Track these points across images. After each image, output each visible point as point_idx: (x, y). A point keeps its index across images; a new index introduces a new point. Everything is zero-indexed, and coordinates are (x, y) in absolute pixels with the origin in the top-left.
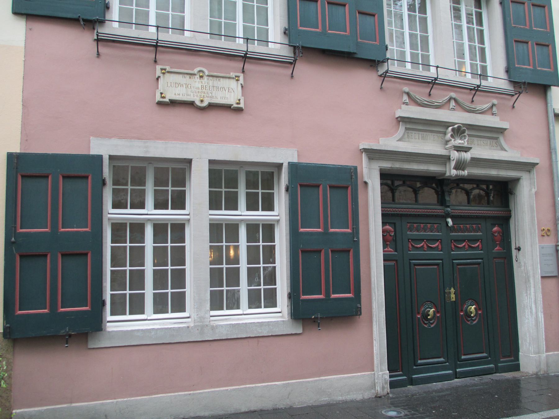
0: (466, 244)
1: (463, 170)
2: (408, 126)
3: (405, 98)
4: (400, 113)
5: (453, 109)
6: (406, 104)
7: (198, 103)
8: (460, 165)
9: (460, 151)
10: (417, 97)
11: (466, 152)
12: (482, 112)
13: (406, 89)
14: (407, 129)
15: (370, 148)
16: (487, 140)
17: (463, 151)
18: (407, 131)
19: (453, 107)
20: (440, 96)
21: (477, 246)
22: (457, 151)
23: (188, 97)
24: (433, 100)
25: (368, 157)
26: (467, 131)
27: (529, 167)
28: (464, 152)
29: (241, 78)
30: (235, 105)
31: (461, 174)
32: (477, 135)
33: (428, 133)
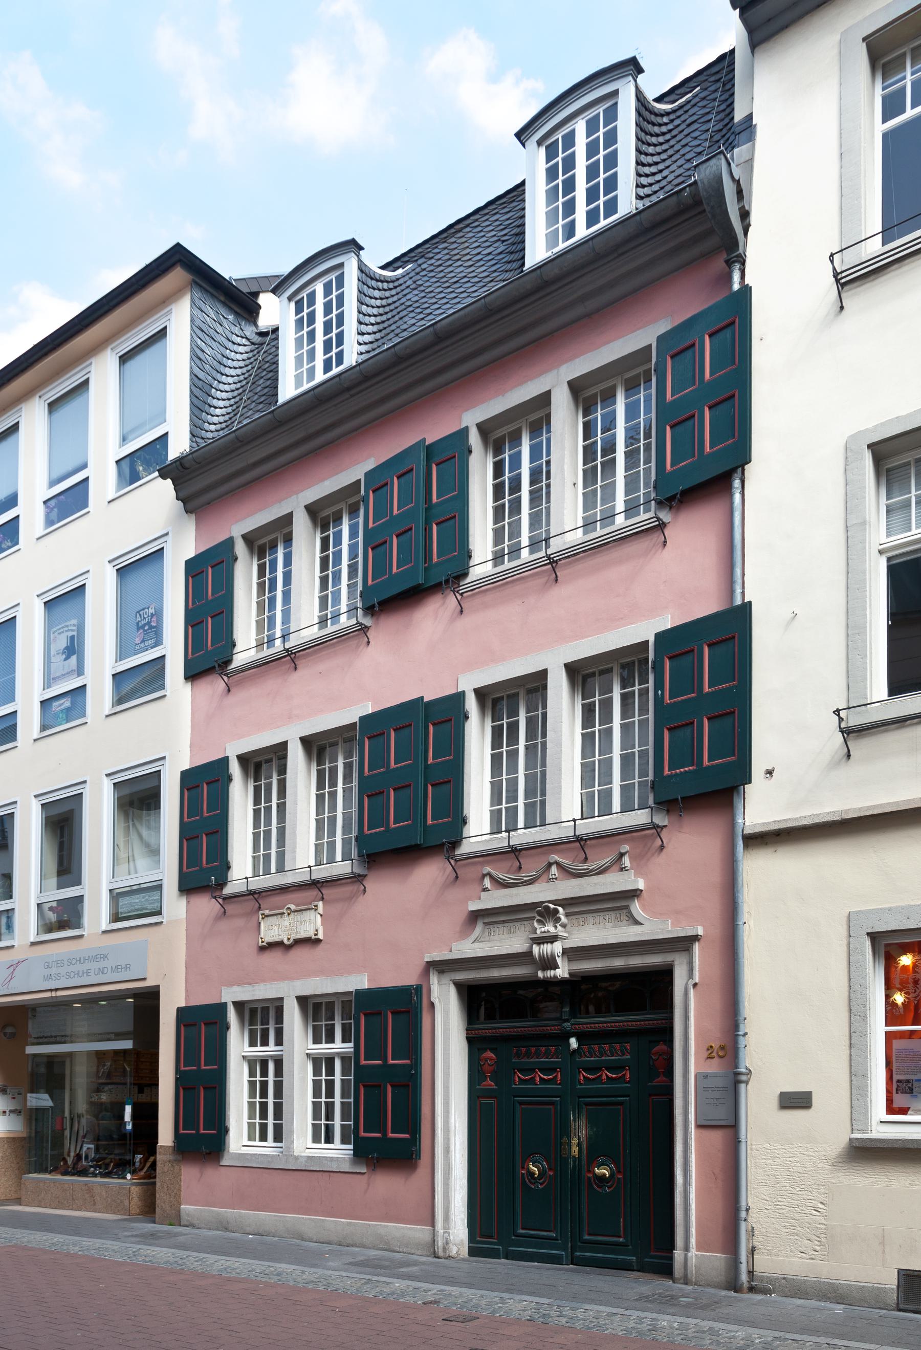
0: (604, 1074)
1: (555, 970)
2: (486, 920)
3: (487, 882)
4: (474, 906)
5: (553, 879)
6: (485, 890)
7: (286, 941)
8: (549, 963)
9: (543, 943)
10: (501, 876)
11: (552, 942)
12: (601, 871)
13: (488, 869)
14: (484, 923)
15: (431, 960)
16: (608, 913)
17: (547, 943)
18: (488, 927)
19: (554, 877)
20: (531, 866)
21: (620, 1078)
22: (539, 944)
23: (280, 937)
24: (524, 875)
25: (437, 970)
26: (560, 909)
27: (684, 944)
28: (549, 945)
29: (320, 904)
30: (313, 937)
31: (549, 976)
32: (589, 910)
33: (515, 924)
